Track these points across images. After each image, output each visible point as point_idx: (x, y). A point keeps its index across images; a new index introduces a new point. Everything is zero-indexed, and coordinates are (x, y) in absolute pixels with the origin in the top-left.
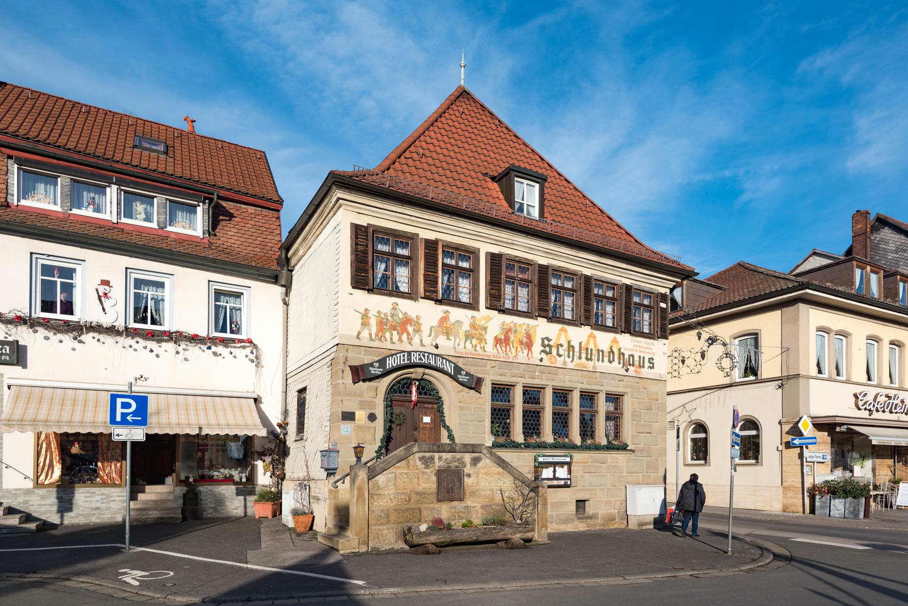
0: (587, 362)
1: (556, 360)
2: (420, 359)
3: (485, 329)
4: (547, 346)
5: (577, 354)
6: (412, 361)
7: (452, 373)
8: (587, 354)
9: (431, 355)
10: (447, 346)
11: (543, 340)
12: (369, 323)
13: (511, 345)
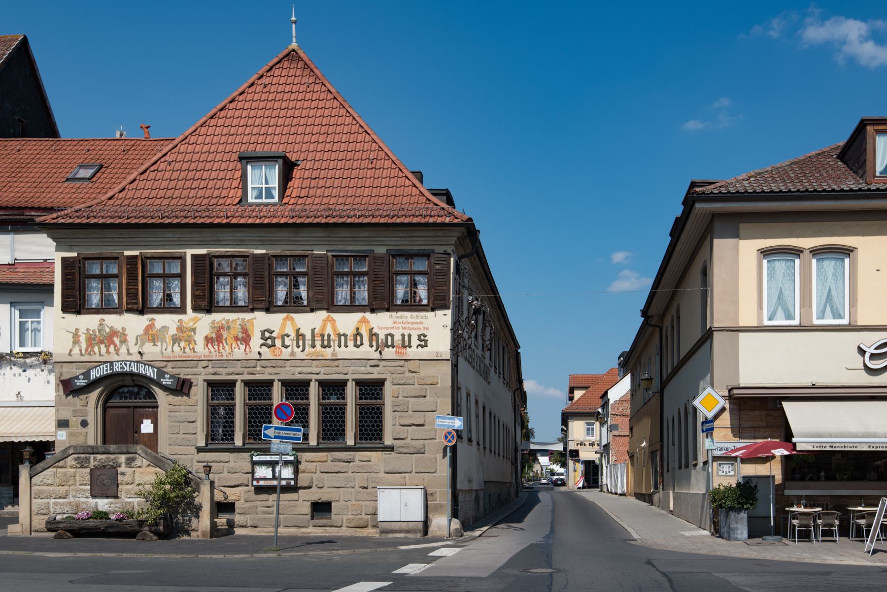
0: (324, 350)
1: (281, 352)
2: (122, 368)
3: (194, 330)
4: (268, 337)
5: (308, 343)
6: (115, 371)
8: (323, 340)
9: (132, 363)
10: (152, 351)
11: (263, 332)
13: (224, 343)
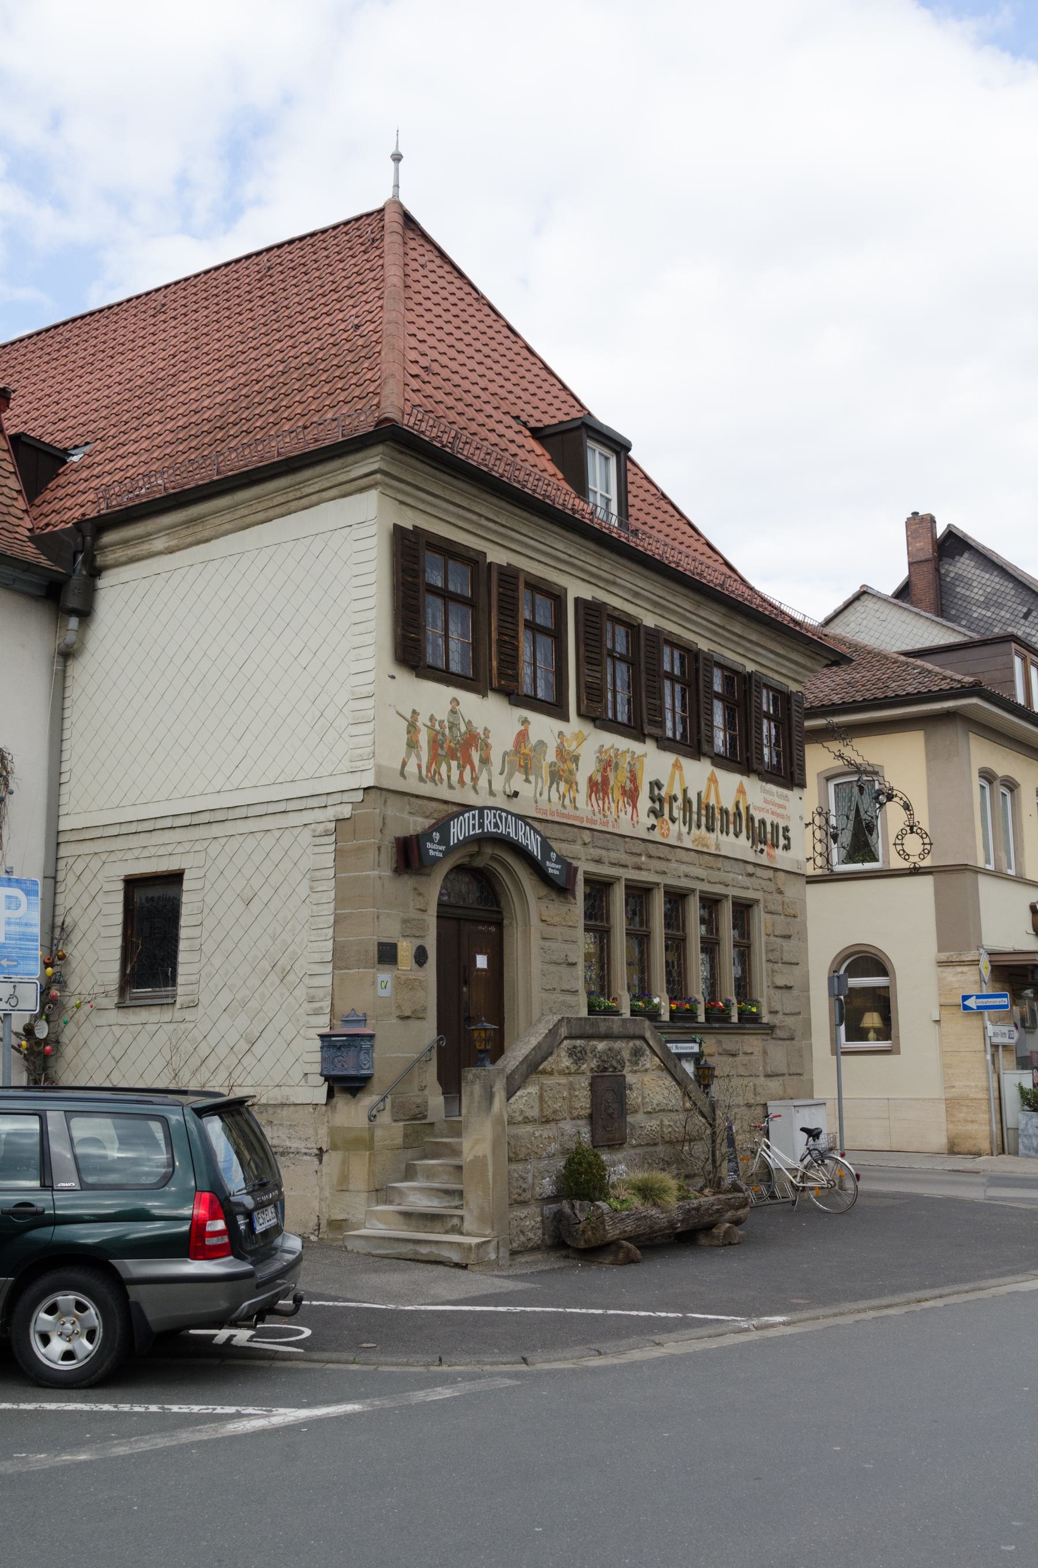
1: (668, 829)
6: (486, 830)
7: (539, 858)
12: (417, 741)
13: (610, 796)
